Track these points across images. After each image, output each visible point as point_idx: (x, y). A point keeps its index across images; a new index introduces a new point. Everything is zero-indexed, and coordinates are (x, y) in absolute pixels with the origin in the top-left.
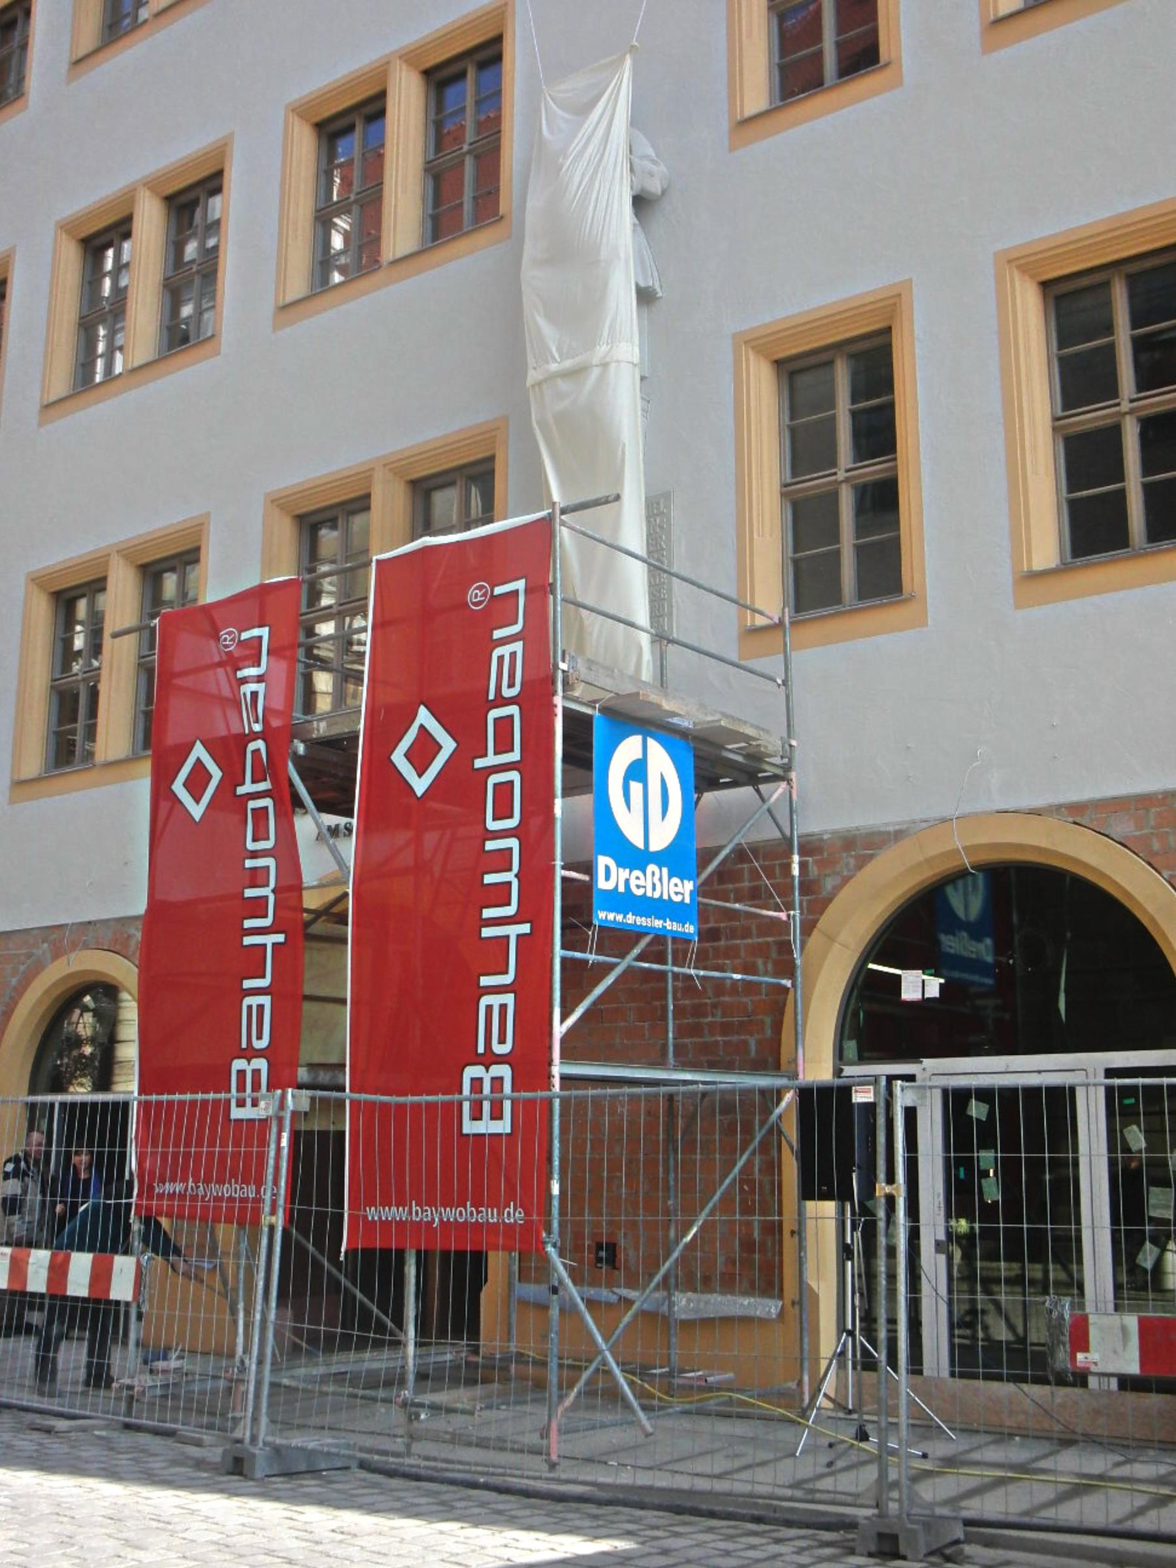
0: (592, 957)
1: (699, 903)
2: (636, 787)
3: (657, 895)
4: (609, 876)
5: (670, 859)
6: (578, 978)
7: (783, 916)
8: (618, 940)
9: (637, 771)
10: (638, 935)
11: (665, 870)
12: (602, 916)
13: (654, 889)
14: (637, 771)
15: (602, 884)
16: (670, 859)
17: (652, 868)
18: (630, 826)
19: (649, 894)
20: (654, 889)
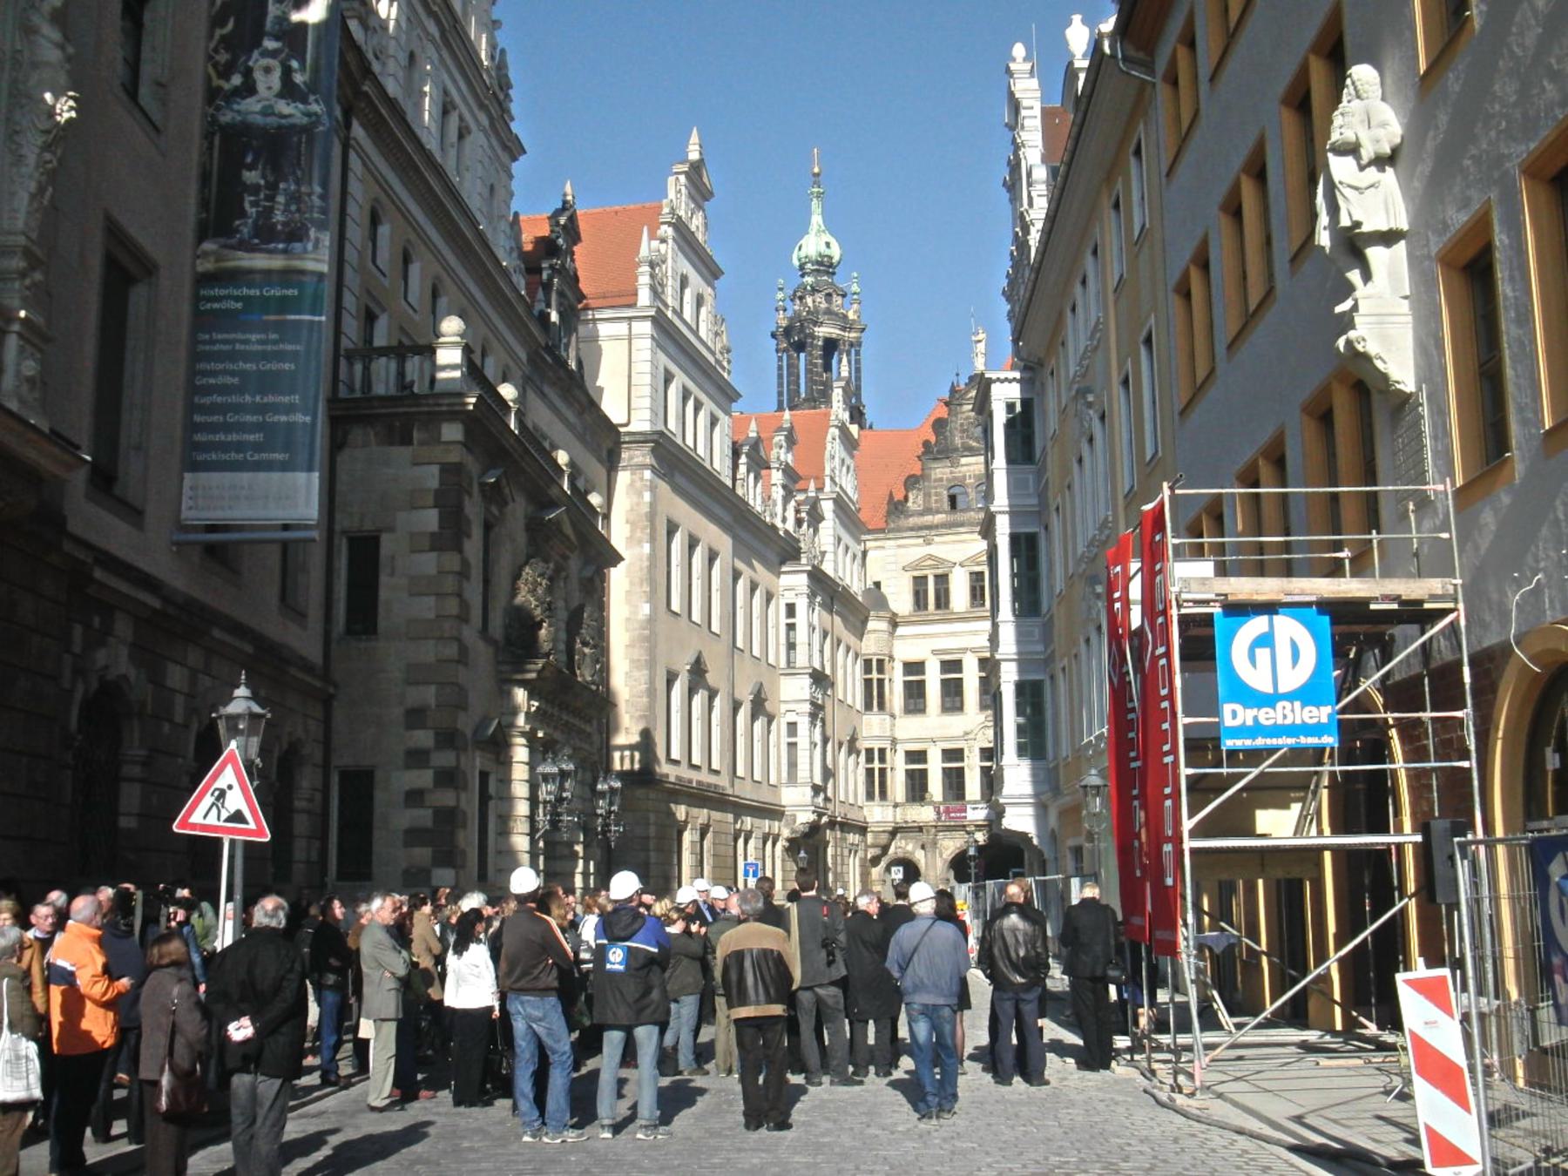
0: (1225, 770)
1: (1340, 721)
2: (1263, 654)
3: (1289, 721)
4: (1233, 715)
5: (1306, 695)
6: (1202, 789)
7: (1458, 714)
8: (1255, 756)
9: (1266, 640)
10: (1271, 751)
11: (1297, 704)
12: (1228, 743)
13: (1285, 717)
14: (1266, 640)
15: (1228, 721)
16: (1306, 695)
17: (1280, 705)
18: (1258, 679)
19: (1280, 721)
20: (1285, 717)
